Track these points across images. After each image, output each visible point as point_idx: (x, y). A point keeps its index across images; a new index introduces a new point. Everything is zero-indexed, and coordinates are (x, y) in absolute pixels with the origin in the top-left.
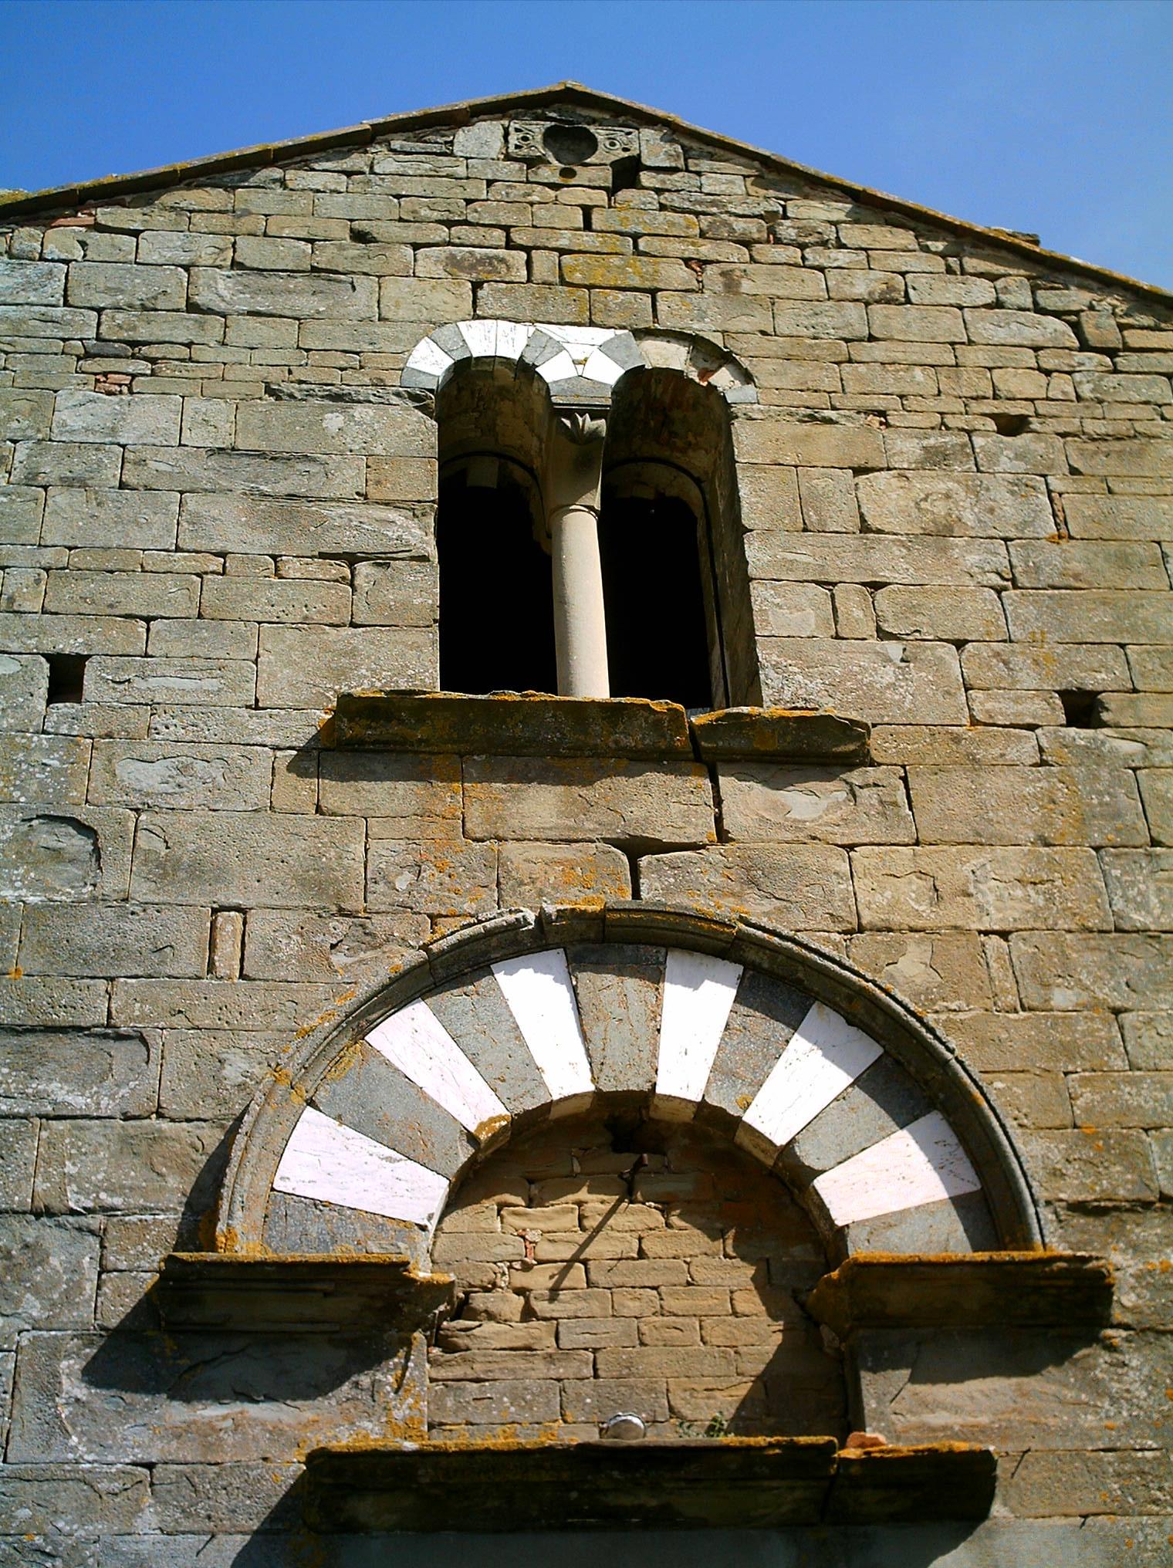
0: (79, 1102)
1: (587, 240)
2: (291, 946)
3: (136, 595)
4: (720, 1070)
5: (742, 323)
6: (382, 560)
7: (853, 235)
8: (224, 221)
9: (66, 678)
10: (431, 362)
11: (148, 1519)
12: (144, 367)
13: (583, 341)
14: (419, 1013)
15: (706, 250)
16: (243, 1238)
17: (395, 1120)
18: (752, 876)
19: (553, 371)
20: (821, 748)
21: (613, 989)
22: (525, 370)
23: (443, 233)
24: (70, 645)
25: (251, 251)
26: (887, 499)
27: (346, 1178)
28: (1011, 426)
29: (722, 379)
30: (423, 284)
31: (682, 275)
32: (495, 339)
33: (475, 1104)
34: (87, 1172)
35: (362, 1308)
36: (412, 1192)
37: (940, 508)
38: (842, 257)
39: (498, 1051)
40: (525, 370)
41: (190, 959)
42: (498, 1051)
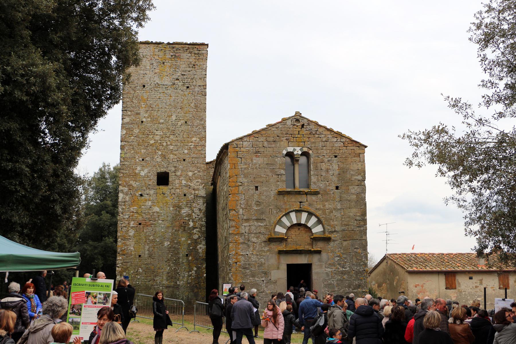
0: (262, 225)
1: (299, 136)
2: (275, 212)
3: (261, 180)
4: (306, 221)
5: (313, 145)
6: (281, 175)
7: (324, 133)
8: (265, 135)
9: (257, 188)
10: (285, 152)
11: (268, 254)
12: (259, 154)
13: (298, 149)
14: (284, 217)
15: (310, 136)
16: (274, 236)
17: (283, 225)
18: (310, 205)
19: (295, 153)
20: (316, 193)
21: (298, 214)
22: (293, 153)
23: (286, 135)
24: (257, 185)
25: (268, 139)
26: (324, 166)
27: (280, 230)
28: (336, 157)
29: (311, 152)
30: (284, 143)
31: (307, 139)
32: (290, 149)
33: (288, 224)
34: (263, 230)
35: (281, 240)
36: (284, 231)
37: (328, 167)
38: (323, 136)
39: (290, 220)
40: (293, 153)
41: (268, 213)
42: (290, 220)
